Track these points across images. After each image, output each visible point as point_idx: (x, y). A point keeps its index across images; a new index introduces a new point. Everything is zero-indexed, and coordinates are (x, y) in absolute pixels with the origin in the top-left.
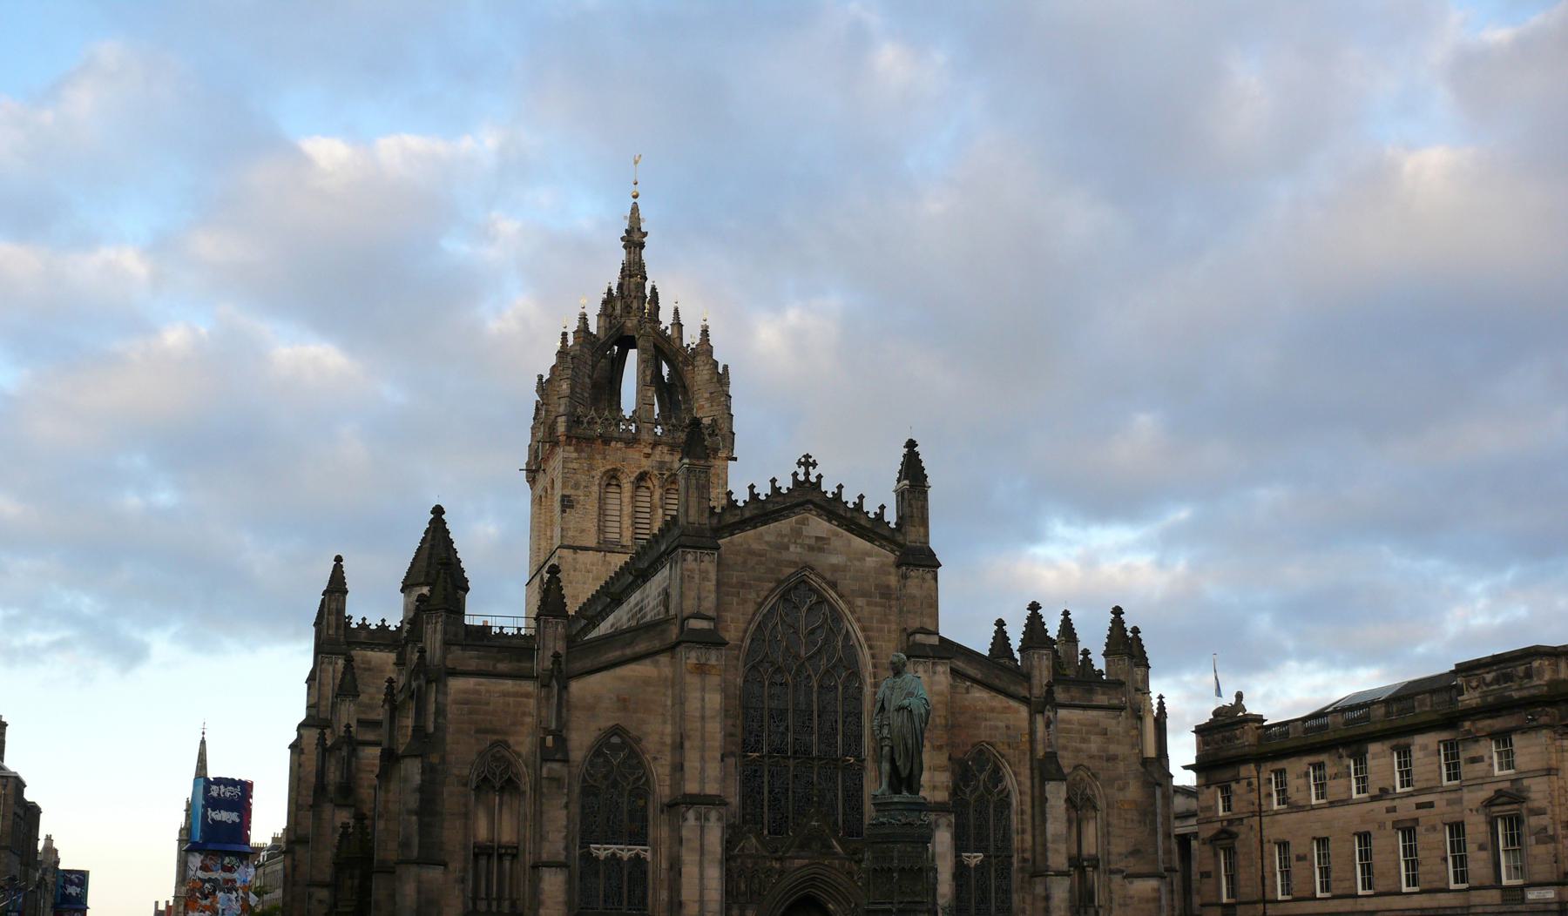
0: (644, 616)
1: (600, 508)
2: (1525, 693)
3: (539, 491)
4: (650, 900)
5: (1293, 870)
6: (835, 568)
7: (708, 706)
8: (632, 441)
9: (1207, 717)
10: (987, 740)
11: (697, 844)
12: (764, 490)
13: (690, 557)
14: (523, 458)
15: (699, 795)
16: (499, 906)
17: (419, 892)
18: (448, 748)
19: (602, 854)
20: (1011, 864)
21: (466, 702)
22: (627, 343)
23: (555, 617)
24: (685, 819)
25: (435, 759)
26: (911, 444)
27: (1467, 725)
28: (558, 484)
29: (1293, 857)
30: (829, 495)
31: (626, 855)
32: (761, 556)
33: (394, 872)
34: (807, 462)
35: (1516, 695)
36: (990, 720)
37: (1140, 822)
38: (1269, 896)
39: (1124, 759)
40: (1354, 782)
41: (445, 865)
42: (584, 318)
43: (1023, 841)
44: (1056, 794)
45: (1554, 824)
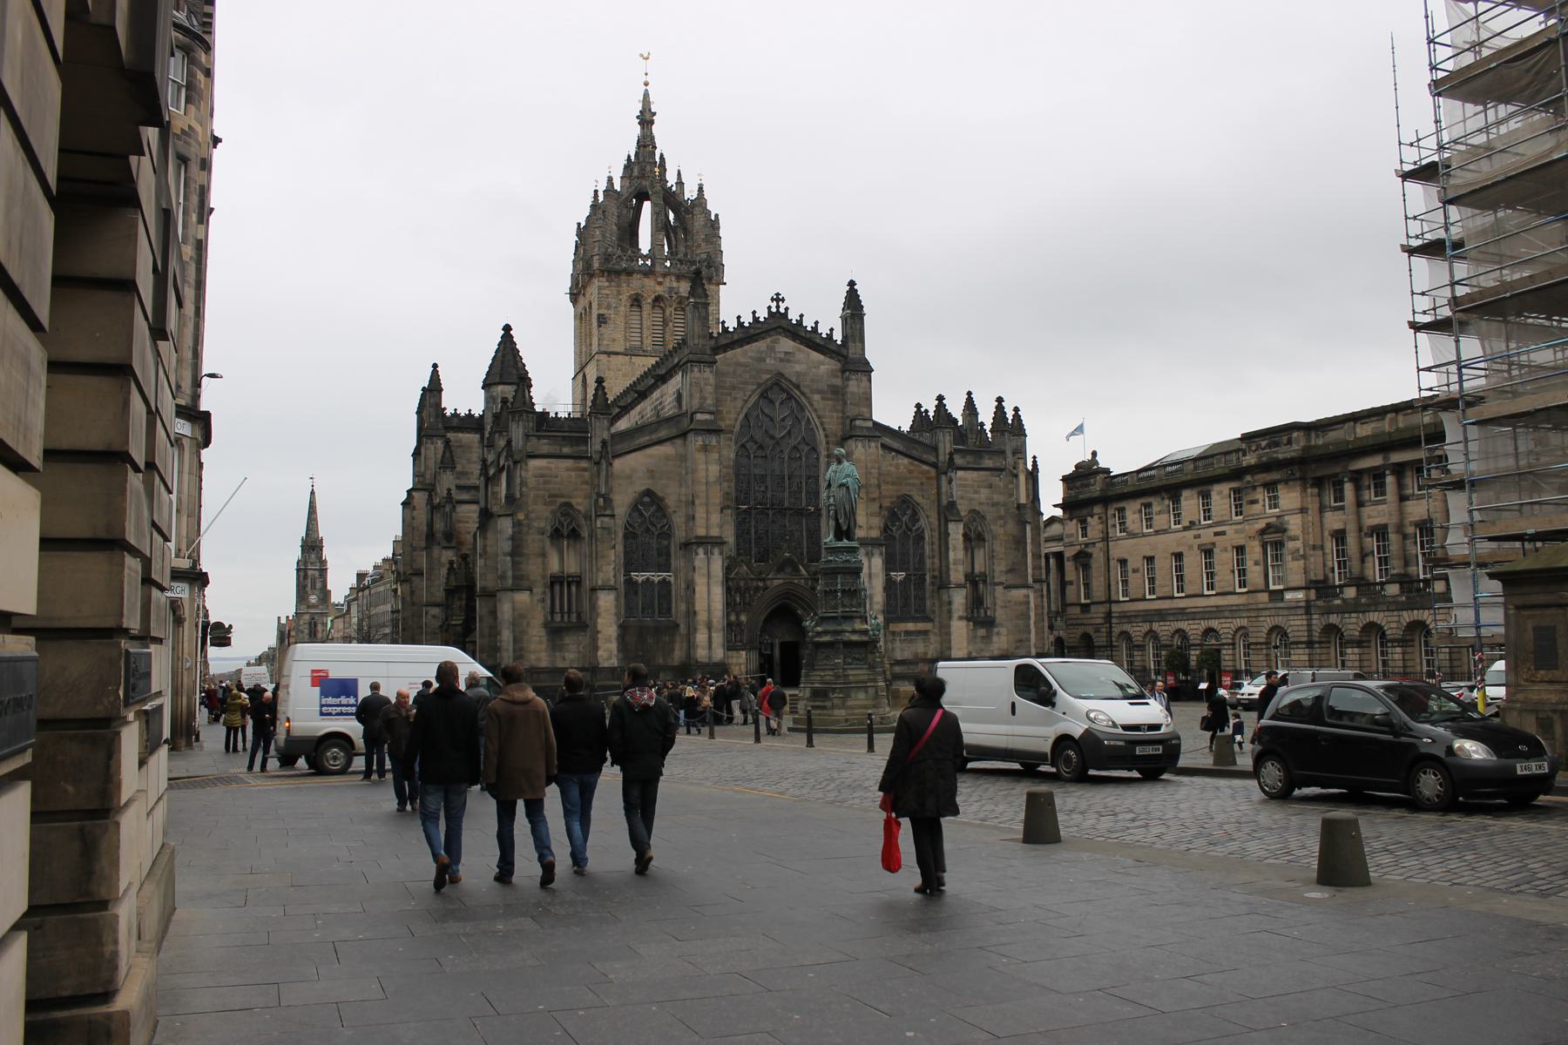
0: (662, 409)
1: (626, 323)
2: (1288, 456)
3: (580, 309)
4: (673, 610)
5: (1130, 579)
6: (798, 374)
7: (711, 474)
8: (648, 272)
9: (1070, 470)
11: (705, 571)
12: (747, 319)
13: (696, 369)
14: (567, 284)
15: (706, 537)
16: (569, 617)
17: (514, 610)
18: (530, 509)
19: (640, 580)
20: (925, 580)
21: (542, 476)
22: (642, 196)
23: (602, 414)
24: (697, 554)
25: (521, 516)
26: (852, 284)
27: (1248, 478)
28: (595, 306)
29: (1130, 570)
30: (794, 322)
31: (656, 580)
33: (495, 596)
34: (778, 299)
35: (1281, 456)
37: (1015, 549)
38: (1114, 598)
39: (1004, 505)
40: (1172, 517)
41: (531, 590)
42: (610, 180)
43: (933, 563)
44: (956, 531)
45: (1304, 546)
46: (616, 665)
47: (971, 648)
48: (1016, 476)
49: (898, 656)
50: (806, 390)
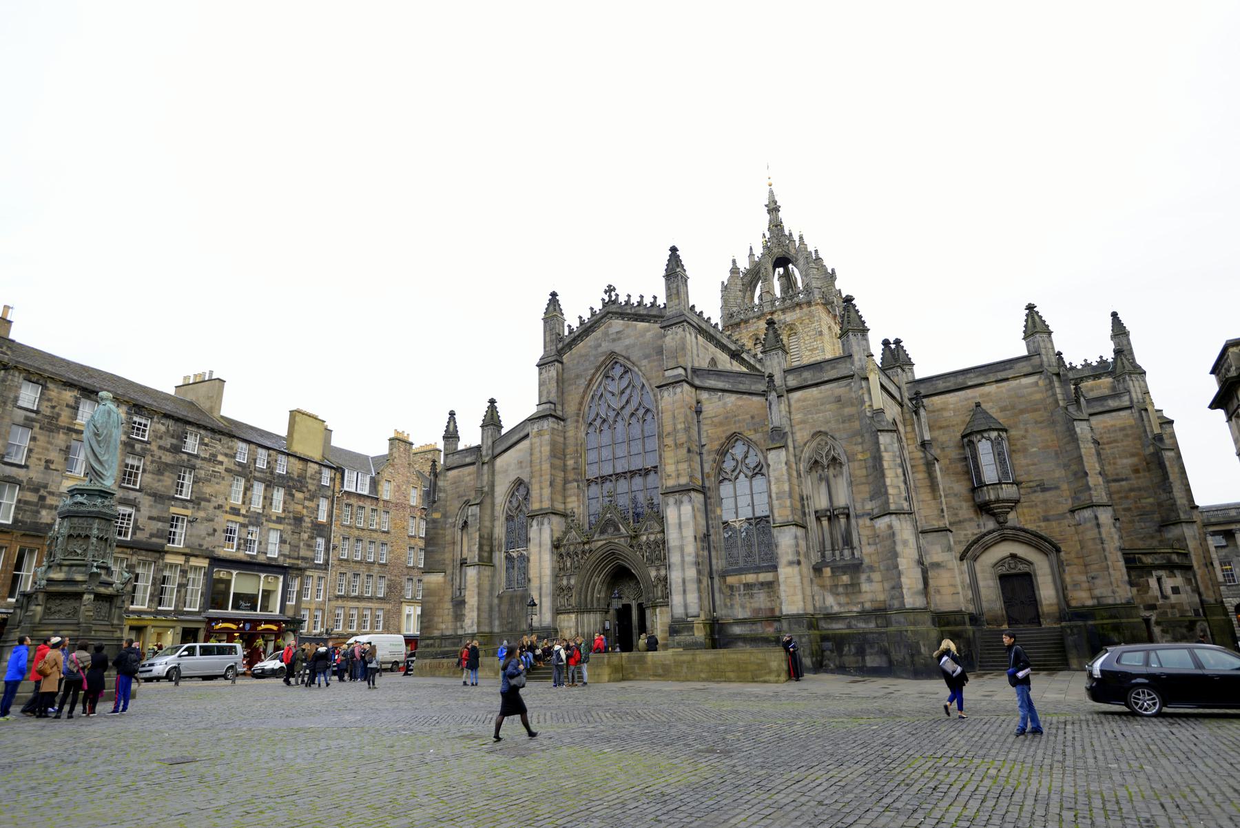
6: (627, 347)
10: (737, 431)
11: (537, 541)
13: (544, 371)
15: (541, 509)
19: (514, 555)
21: (455, 483)
23: (487, 426)
24: (532, 526)
26: (674, 250)
32: (586, 356)
36: (739, 415)
42: (734, 261)
46: (476, 631)
47: (830, 600)
48: (867, 379)
49: (740, 614)
50: (633, 358)
